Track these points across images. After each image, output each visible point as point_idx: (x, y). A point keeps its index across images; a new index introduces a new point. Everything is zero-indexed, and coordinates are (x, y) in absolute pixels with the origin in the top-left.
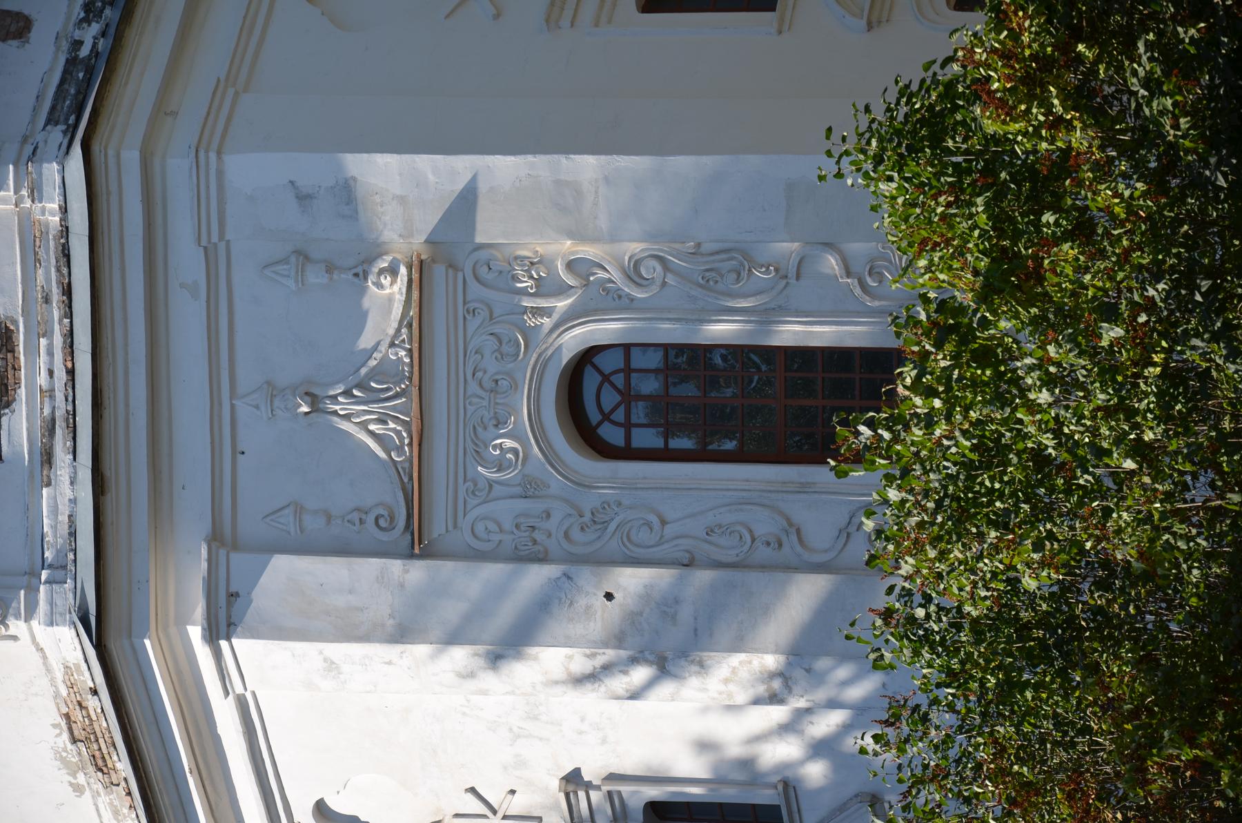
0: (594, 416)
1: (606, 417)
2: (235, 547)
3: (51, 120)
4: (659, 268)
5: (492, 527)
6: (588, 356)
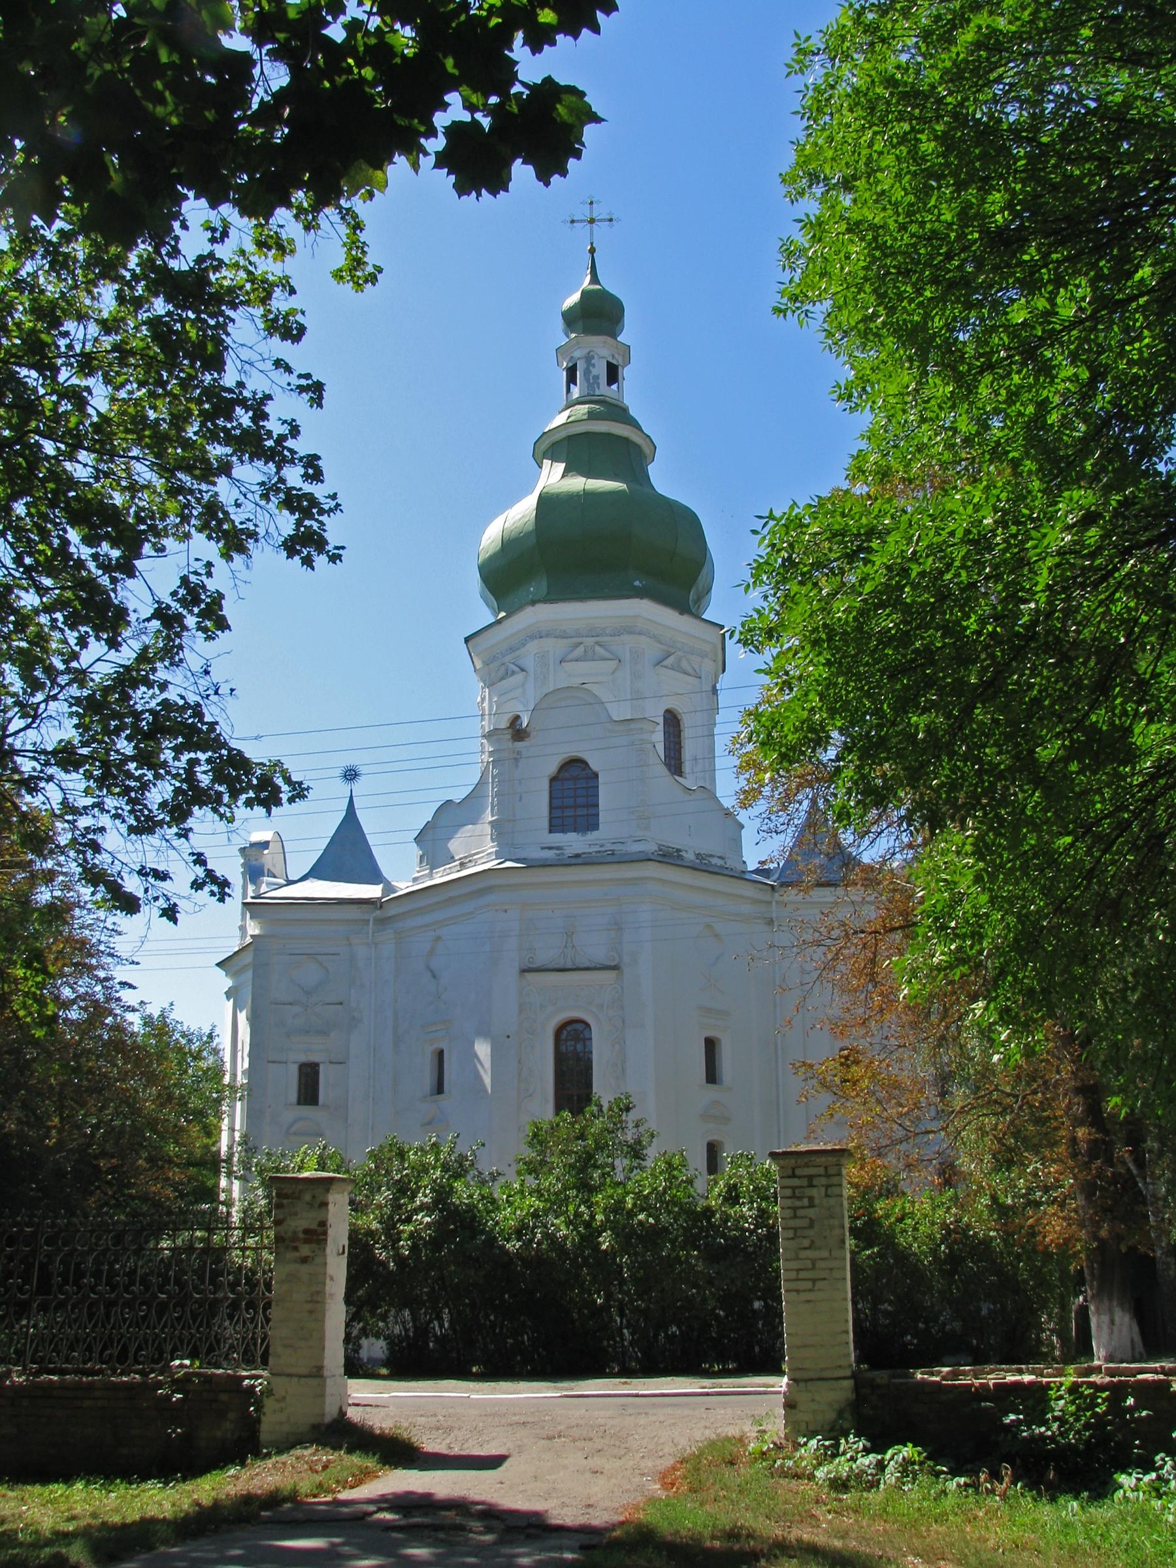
6: (587, 1025)
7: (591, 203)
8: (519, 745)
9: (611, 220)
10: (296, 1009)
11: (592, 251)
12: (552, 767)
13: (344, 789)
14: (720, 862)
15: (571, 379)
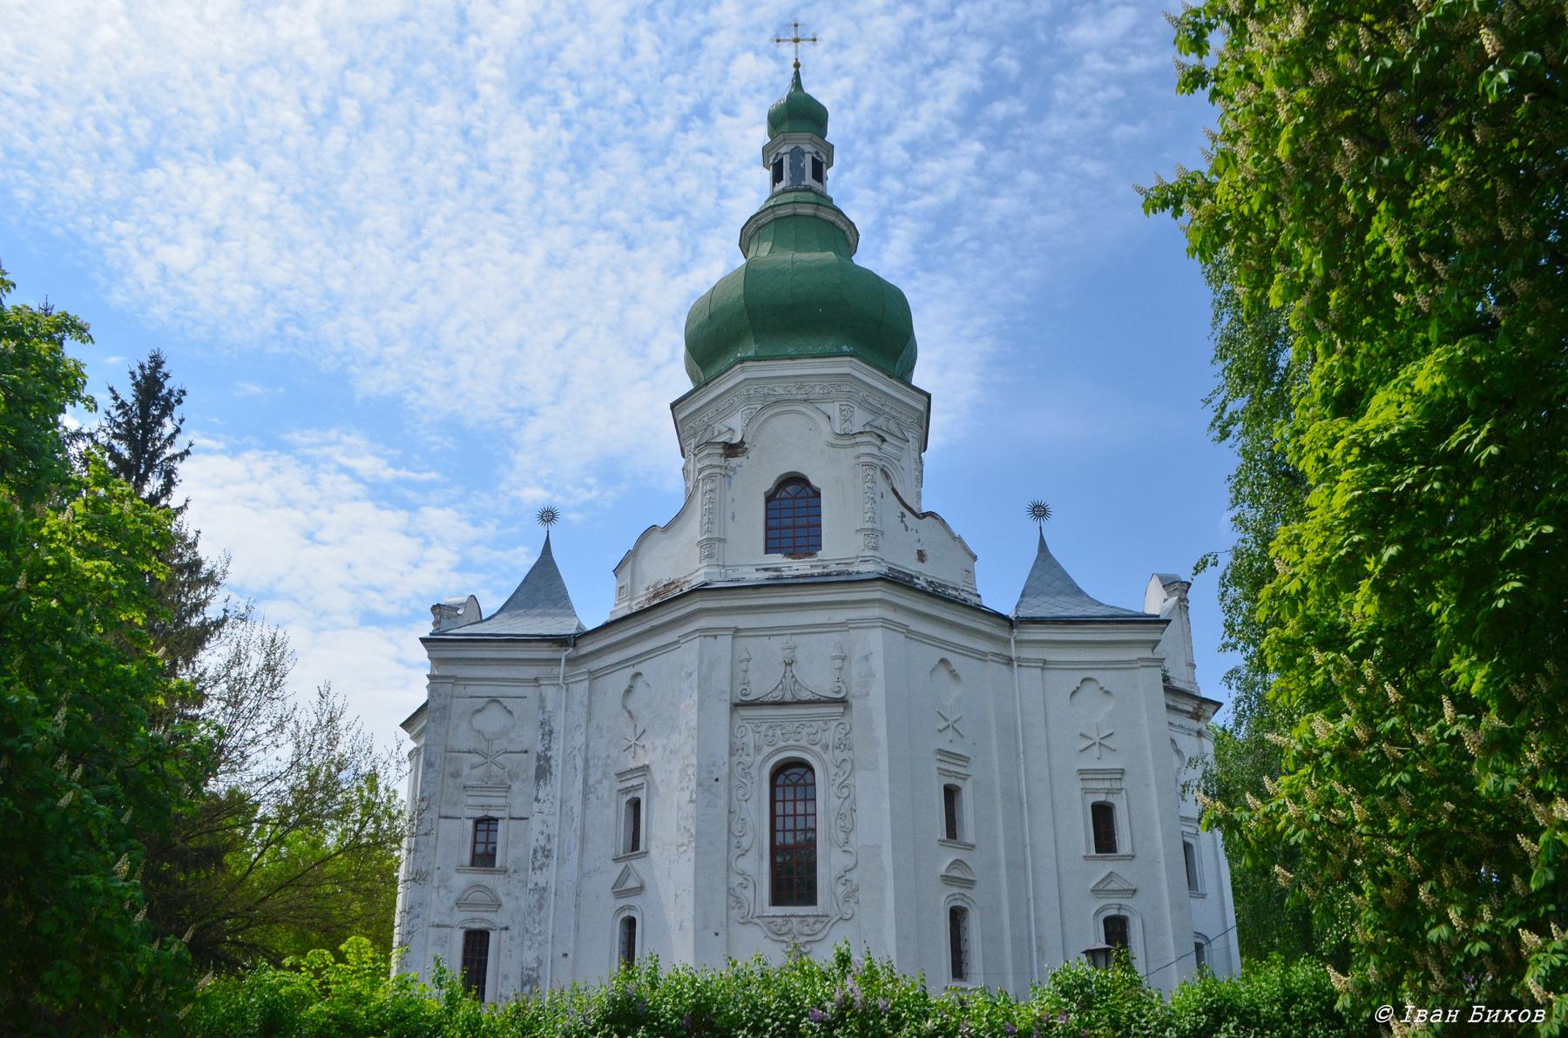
0: (787, 773)
1: (787, 777)
2: (734, 637)
3: (890, 569)
6: (810, 769)
7: (796, 25)
8: (733, 461)
9: (815, 40)
10: (477, 759)
11: (797, 65)
12: (769, 484)
13: (540, 530)
14: (954, 593)
15: (777, 177)
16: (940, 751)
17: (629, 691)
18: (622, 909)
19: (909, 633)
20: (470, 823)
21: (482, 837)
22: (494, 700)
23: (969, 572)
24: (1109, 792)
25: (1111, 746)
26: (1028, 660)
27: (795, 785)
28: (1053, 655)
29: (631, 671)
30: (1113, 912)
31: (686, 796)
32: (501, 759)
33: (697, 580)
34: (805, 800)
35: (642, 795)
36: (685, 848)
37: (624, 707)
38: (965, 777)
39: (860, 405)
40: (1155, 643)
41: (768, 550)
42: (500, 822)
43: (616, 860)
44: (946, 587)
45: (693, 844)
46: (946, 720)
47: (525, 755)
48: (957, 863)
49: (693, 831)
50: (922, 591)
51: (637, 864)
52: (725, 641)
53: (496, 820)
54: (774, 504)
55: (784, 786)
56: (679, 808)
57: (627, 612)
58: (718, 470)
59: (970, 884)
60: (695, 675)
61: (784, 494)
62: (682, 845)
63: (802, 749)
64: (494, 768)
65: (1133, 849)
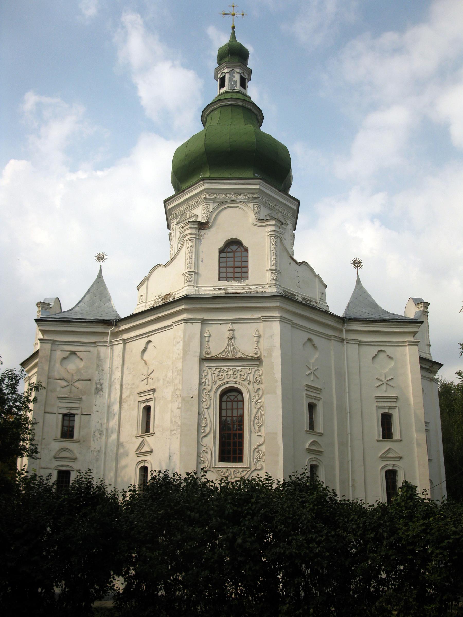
0: (228, 395)
1: (228, 397)
2: (202, 324)
4: (259, 407)
5: (206, 374)
7: (233, 7)
8: (203, 232)
11: (233, 28)
12: (221, 244)
14: (315, 304)
16: (307, 386)
17: (144, 351)
18: (140, 462)
19: (293, 325)
20: (60, 417)
21: (66, 423)
22: (73, 353)
23: (323, 294)
24: (390, 408)
25: (393, 385)
26: (352, 340)
27: (232, 401)
28: (364, 338)
29: (146, 340)
30: (390, 468)
31: (176, 405)
32: (77, 384)
33: (183, 293)
34: (238, 409)
35: (151, 404)
36: (175, 432)
37: (142, 358)
38: (319, 399)
39: (264, 205)
40: (415, 334)
41: (220, 279)
42: (76, 416)
43: (138, 437)
44: (310, 301)
45: (179, 430)
46: (310, 369)
47: (89, 382)
48: (314, 443)
49: (179, 423)
50: (300, 303)
51: (149, 439)
52: (197, 326)
53: (74, 415)
54: (223, 255)
55: (227, 401)
56: (172, 411)
57: (143, 309)
58: (194, 236)
59: (320, 453)
60: (181, 344)
61: (229, 250)
62: (173, 430)
63: (237, 383)
64: (73, 388)
65: (401, 437)
